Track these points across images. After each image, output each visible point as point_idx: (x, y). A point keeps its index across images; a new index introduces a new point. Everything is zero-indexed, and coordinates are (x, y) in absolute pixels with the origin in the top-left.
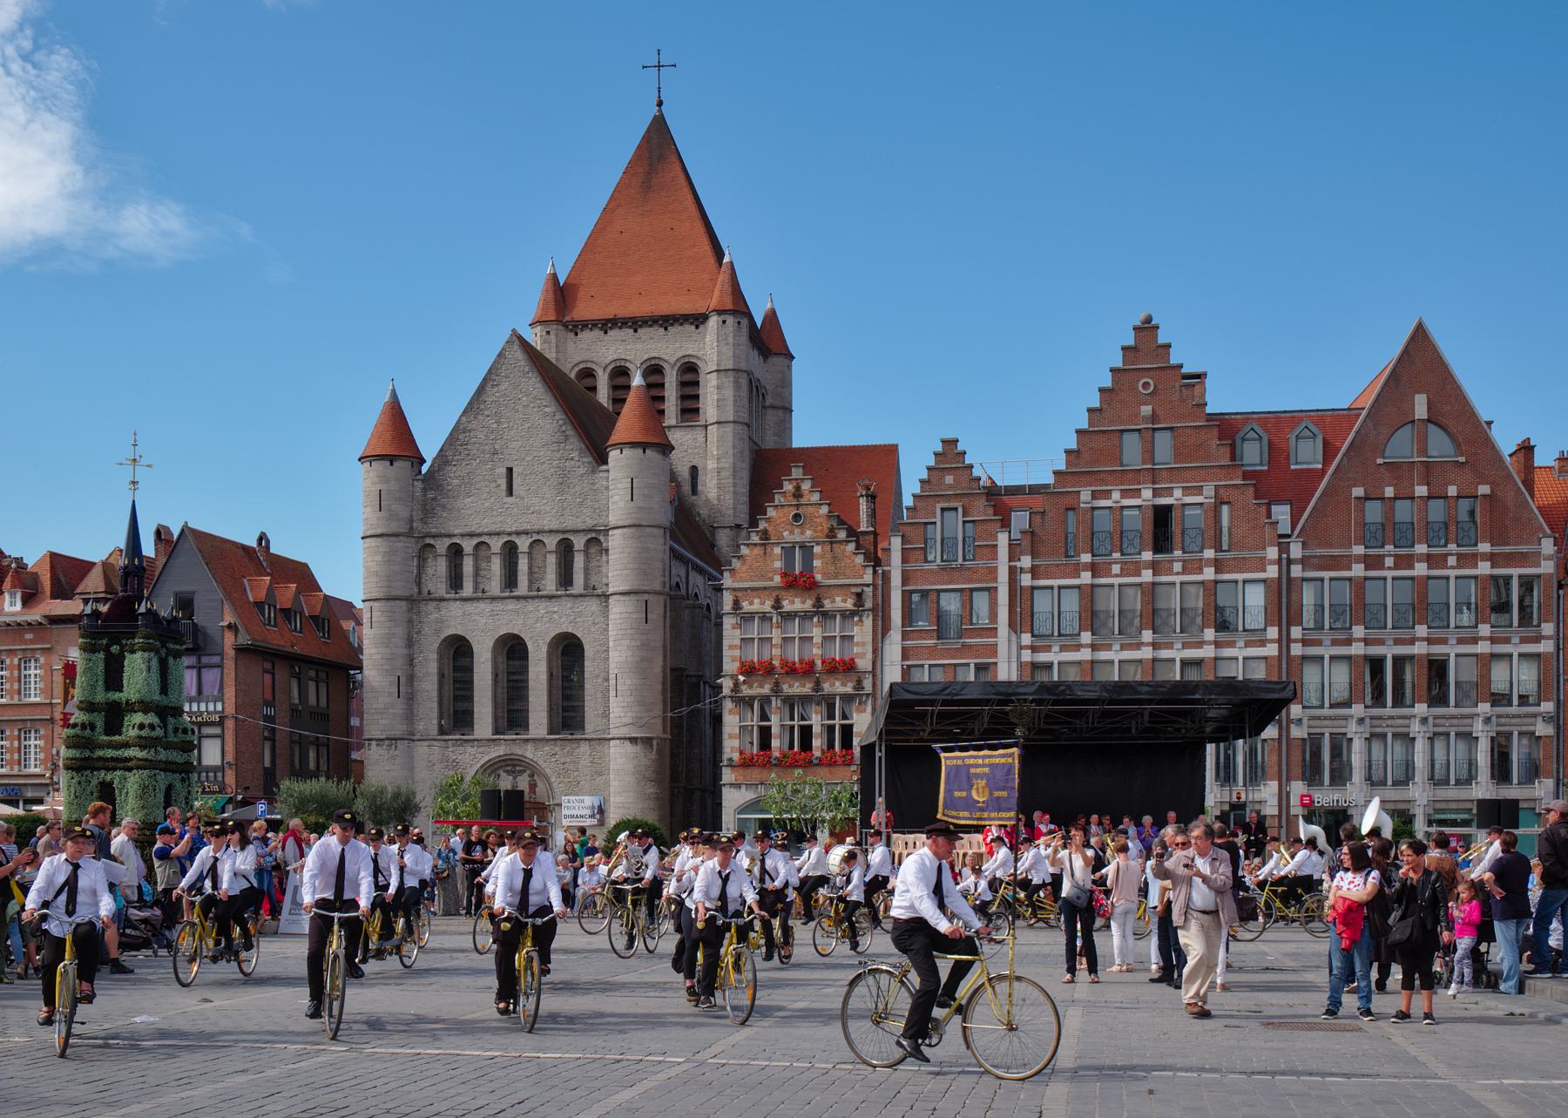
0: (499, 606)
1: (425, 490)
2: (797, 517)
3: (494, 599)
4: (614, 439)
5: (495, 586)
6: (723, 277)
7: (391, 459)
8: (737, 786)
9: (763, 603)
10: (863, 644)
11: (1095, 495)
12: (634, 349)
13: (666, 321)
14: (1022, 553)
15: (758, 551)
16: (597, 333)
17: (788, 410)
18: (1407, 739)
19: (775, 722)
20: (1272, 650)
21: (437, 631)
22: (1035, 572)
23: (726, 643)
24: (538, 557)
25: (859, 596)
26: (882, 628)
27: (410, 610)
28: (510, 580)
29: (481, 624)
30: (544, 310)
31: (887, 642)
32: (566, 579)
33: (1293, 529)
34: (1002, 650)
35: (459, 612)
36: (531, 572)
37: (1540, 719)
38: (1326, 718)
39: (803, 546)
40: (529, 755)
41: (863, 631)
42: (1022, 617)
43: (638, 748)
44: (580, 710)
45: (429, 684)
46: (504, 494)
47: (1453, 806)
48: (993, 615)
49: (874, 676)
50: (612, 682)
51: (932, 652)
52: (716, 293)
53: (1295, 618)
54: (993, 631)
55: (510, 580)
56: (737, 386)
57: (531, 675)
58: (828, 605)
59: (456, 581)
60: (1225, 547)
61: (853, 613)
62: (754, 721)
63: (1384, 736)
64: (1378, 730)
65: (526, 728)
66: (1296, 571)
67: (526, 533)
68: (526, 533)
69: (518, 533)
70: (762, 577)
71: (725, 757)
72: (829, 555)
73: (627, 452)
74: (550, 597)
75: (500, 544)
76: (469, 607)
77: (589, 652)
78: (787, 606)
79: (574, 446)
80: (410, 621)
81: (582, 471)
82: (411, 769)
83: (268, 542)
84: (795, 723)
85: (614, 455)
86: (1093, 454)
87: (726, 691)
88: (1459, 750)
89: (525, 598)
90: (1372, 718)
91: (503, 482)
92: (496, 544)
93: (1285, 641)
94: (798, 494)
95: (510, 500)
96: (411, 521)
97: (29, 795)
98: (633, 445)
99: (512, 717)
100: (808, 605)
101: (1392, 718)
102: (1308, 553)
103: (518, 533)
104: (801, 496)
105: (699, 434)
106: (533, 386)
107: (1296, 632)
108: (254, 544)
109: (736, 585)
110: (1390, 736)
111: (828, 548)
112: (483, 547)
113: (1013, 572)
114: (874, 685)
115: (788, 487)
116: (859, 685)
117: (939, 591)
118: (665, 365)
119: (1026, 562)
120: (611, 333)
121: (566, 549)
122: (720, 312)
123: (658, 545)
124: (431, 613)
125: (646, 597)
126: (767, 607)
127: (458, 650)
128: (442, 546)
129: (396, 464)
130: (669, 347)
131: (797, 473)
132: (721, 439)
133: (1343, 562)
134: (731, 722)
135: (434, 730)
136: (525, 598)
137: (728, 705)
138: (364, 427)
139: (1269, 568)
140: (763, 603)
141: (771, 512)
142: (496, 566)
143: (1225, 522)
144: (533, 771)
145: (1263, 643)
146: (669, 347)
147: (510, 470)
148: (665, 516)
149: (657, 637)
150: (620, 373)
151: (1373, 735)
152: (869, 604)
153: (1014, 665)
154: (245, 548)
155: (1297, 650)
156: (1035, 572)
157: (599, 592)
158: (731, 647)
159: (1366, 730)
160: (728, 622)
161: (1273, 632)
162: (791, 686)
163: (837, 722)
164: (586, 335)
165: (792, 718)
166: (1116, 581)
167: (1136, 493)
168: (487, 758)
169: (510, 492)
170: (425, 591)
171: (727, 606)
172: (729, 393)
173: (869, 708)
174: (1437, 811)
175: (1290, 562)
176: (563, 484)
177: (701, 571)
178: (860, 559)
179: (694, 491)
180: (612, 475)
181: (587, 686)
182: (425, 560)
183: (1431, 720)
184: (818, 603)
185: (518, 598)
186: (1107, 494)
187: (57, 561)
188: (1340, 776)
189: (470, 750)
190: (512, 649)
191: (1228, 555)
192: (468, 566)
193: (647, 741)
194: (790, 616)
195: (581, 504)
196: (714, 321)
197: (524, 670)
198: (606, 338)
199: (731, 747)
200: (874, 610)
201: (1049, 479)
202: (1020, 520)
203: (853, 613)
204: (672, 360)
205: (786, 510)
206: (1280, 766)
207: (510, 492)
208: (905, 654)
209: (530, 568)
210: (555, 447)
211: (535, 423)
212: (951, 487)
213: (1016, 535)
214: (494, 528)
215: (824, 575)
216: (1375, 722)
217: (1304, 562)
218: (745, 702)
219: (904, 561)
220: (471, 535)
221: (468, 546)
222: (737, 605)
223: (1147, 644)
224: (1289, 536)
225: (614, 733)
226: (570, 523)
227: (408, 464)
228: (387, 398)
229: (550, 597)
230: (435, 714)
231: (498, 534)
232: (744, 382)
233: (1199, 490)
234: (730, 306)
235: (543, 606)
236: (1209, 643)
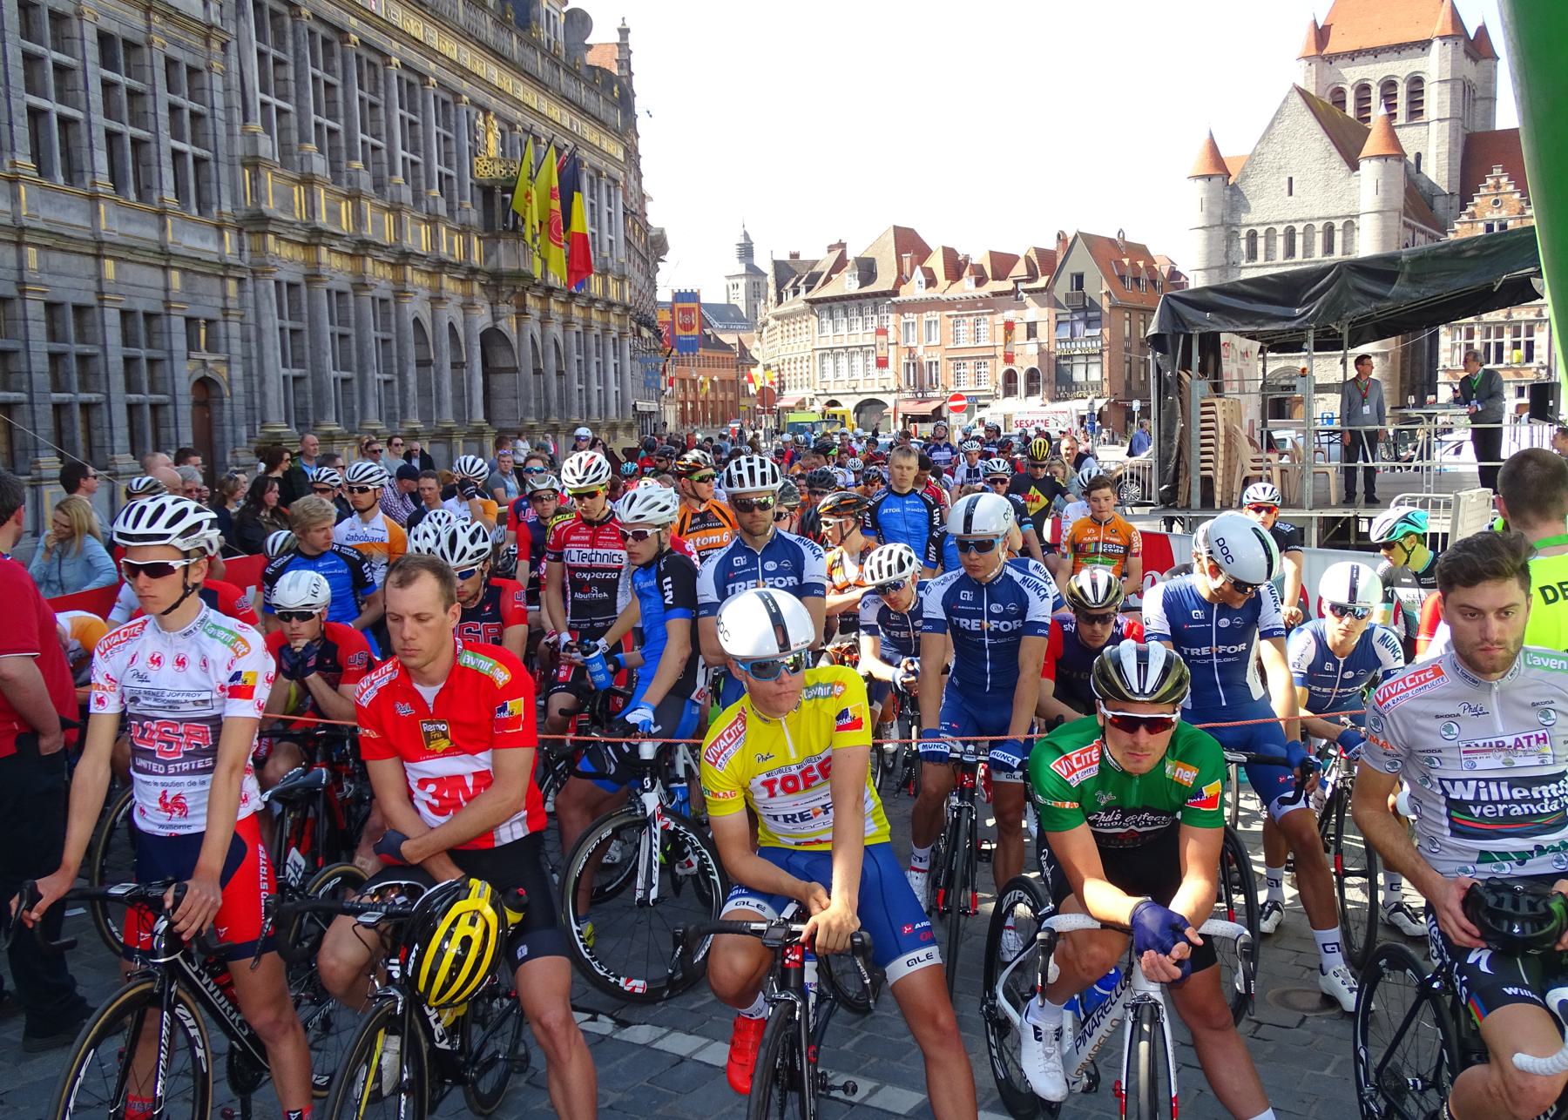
2: (1496, 202)
4: (1366, 151)
7: (1209, 177)
12: (1373, 72)
13: (1399, 49)
16: (1347, 61)
30: (1308, 47)
39: (1499, 220)
52: (1439, 23)
56: (1453, 89)
73: (1374, 162)
79: (1337, 156)
85: (1364, 164)
91: (1286, 187)
92: (1280, 229)
94: (1497, 186)
97: (981, 402)
98: (1378, 157)
105: (1424, 129)
106: (1309, 120)
115: (1490, 182)
116: (1540, 314)
122: (1441, 38)
123: (1396, 222)
128: (1244, 232)
130: (1399, 69)
131: (1497, 171)
132: (1440, 131)
141: (1477, 200)
142: (1280, 243)
146: (1399, 69)
148: (1399, 200)
150: (1363, 89)
154: (1111, 241)
163: (1523, 339)
165: (1488, 336)
169: (1291, 193)
172: (1447, 97)
176: (1327, 186)
177: (1423, 232)
179: (1418, 171)
187: (994, 255)
192: (1261, 244)
196: (1437, 44)
207: (1291, 193)
211: (1309, 143)
214: (1279, 218)
221: (1261, 231)
228: (1207, 136)
232: (1459, 87)
234: (1449, 32)
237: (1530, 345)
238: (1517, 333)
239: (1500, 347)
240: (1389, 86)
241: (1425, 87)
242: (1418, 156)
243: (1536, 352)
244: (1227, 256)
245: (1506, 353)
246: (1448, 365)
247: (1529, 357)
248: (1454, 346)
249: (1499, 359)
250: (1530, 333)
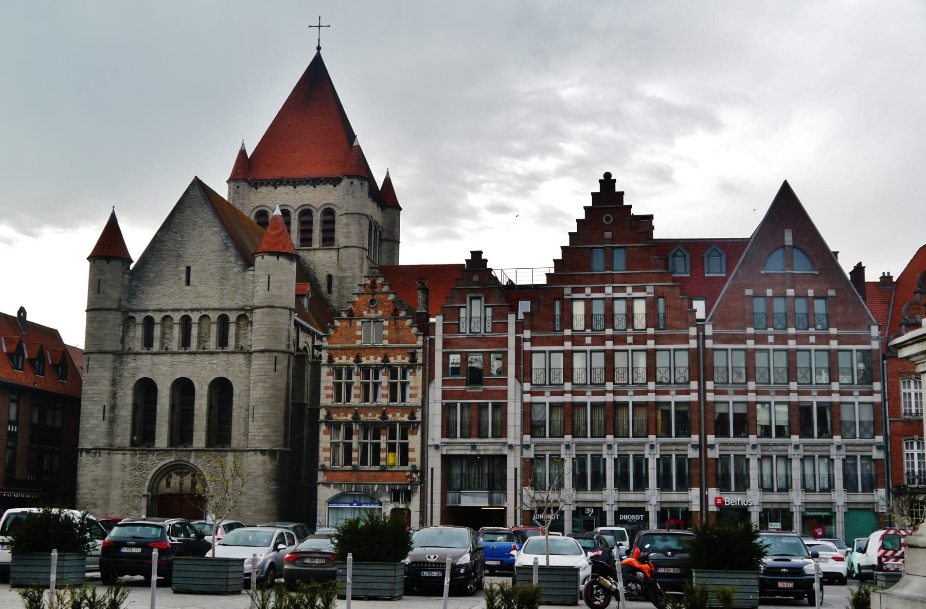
0: (177, 358)
1: (130, 280)
2: (372, 301)
3: (174, 353)
5: (174, 345)
8: (327, 484)
9: (348, 359)
10: (416, 388)
11: (574, 291)
13: (315, 182)
14: (524, 328)
15: (345, 323)
17: (397, 242)
18: (787, 460)
19: (355, 441)
21: (134, 375)
23: (323, 385)
24: (205, 326)
25: (413, 356)
26: (428, 378)
27: (115, 361)
28: (185, 341)
29: (164, 371)
31: (432, 386)
32: (223, 341)
33: (707, 315)
34: (511, 394)
35: (149, 362)
36: (199, 336)
37: (874, 448)
38: (731, 444)
40: (192, 461)
41: (415, 379)
42: (525, 373)
43: (266, 458)
44: (228, 431)
45: (126, 412)
46: (184, 283)
47: (819, 506)
48: (503, 371)
49: (423, 411)
50: (251, 411)
51: (463, 395)
53: (709, 376)
54: (505, 382)
55: (185, 341)
57: (196, 406)
58: (392, 360)
59: (148, 341)
60: (661, 327)
61: (409, 367)
62: (341, 438)
63: (771, 457)
64: (766, 453)
65: (192, 443)
66: (709, 344)
67: (197, 310)
68: (197, 310)
69: (192, 310)
70: (348, 341)
71: (320, 463)
72: (393, 327)
74: (212, 353)
75: (179, 317)
76: (157, 359)
77: (236, 391)
78: (364, 361)
80: (115, 368)
81: (237, 270)
82: (110, 470)
83: (25, 313)
84: (368, 441)
85: (258, 259)
86: (573, 263)
87: (322, 418)
88: (822, 469)
89: (195, 353)
90: (762, 445)
91: (184, 276)
92: (177, 317)
93: (702, 391)
95: (187, 288)
96: (120, 301)
100: (379, 360)
101: (775, 445)
102: (717, 331)
103: (192, 310)
104: (376, 287)
105: (334, 253)
107: (710, 385)
108: (15, 314)
109: (330, 346)
110: (774, 457)
111: (393, 322)
112: (169, 319)
113: (518, 340)
114: (423, 416)
116: (412, 416)
117: (467, 352)
118: (313, 210)
119: (527, 334)
120: (279, 188)
121: (223, 322)
122: (350, 177)
124: (131, 362)
125: (276, 354)
126: (351, 361)
127: (146, 389)
128: (140, 318)
129: (112, 263)
134: (325, 440)
135: (127, 442)
136: (195, 353)
137: (323, 427)
138: (90, 235)
139: (691, 341)
140: (348, 359)
142: (176, 332)
143: (661, 309)
144: (194, 471)
145: (688, 392)
147: (188, 269)
149: (282, 382)
151: (763, 457)
152: (420, 361)
153: (519, 405)
155: (710, 397)
157: (246, 348)
158: (326, 388)
159: (758, 452)
160: (324, 370)
161: (694, 385)
162: (366, 415)
163: (398, 441)
164: (264, 190)
165: (366, 437)
166: (589, 348)
167: (602, 290)
168: (162, 463)
169: (188, 282)
170: (127, 347)
171: (324, 360)
173: (419, 432)
174: (807, 510)
175: (705, 337)
176: (223, 279)
178: (414, 330)
180: (256, 273)
181: (234, 414)
182: (128, 327)
183: (801, 447)
184: (386, 359)
185: (190, 353)
186: (582, 291)
188: (743, 484)
189: (152, 457)
190: (184, 388)
191: (663, 332)
193: (272, 453)
194: (365, 370)
195: (235, 292)
196: (345, 182)
197: (192, 403)
198: (276, 191)
199: (324, 457)
200: (423, 364)
201: (543, 281)
202: (525, 306)
203: (409, 367)
204: (318, 207)
205: (365, 296)
206: (701, 477)
207: (188, 282)
208: (445, 395)
209: (199, 334)
210: (220, 254)
212: (476, 283)
213: (521, 316)
214: (177, 306)
215: (390, 341)
216: (764, 448)
217: (716, 338)
218: (334, 426)
219: (444, 332)
220: (161, 311)
221: (158, 317)
222: (331, 360)
223: (610, 392)
224: (703, 320)
225: (252, 447)
226: (227, 304)
227: (120, 263)
229: (212, 353)
230: (128, 432)
231: (178, 310)
233: (643, 289)
235: (206, 359)
236: (652, 391)
237: (405, 449)
238: (392, 436)
239: (377, 447)
240: (306, 213)
241: (337, 219)
242: (330, 277)
243: (410, 455)
244: (123, 341)
245: (383, 455)
246: (328, 464)
247: (404, 460)
248: (335, 445)
249: (376, 461)
250: (404, 436)
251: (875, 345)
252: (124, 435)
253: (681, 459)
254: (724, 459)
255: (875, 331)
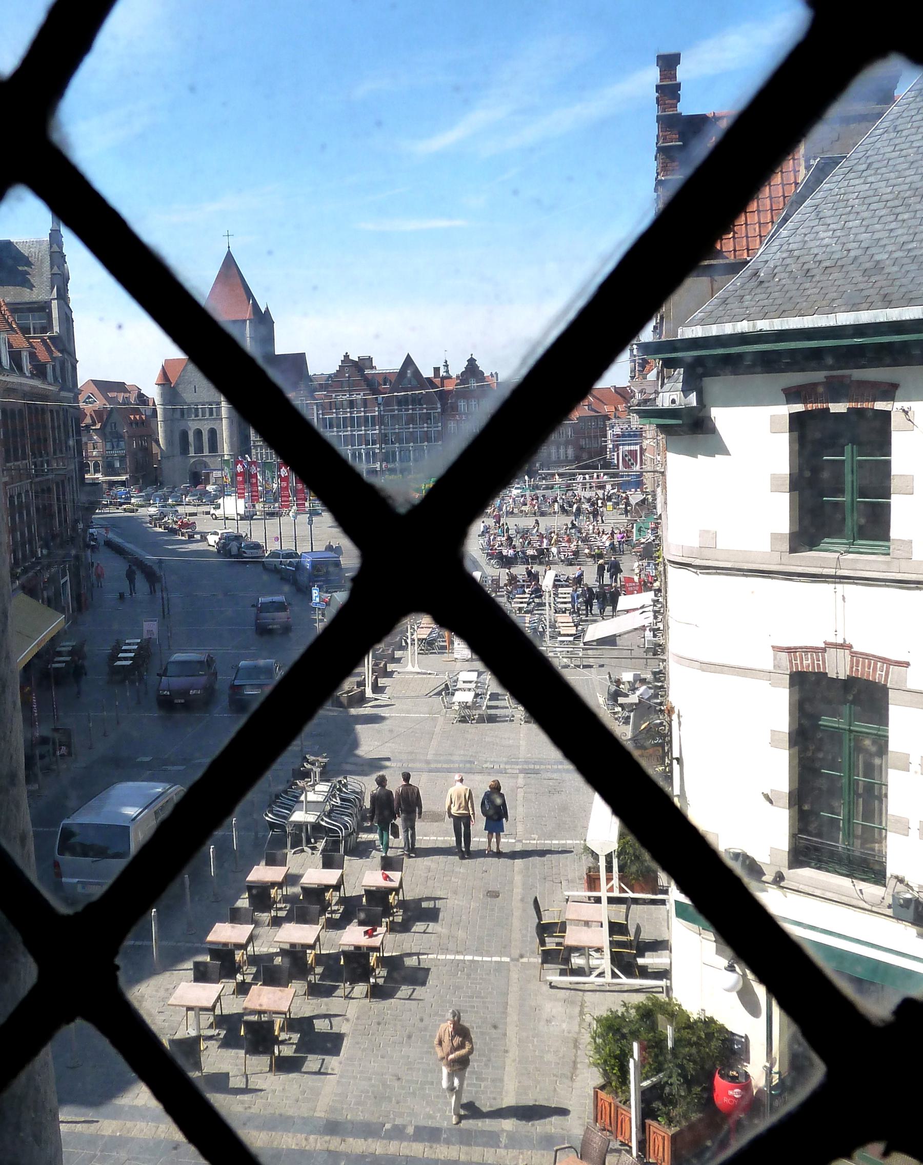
6: (250, 308)
20: (377, 432)
22: (323, 414)
93: (380, 429)
99: (199, 449)
133: (393, 410)
156: (323, 414)
188: (394, 460)
190: (199, 433)
251: (439, 410)
252: (177, 450)
253: (374, 453)
254: (387, 452)
255: (439, 406)
